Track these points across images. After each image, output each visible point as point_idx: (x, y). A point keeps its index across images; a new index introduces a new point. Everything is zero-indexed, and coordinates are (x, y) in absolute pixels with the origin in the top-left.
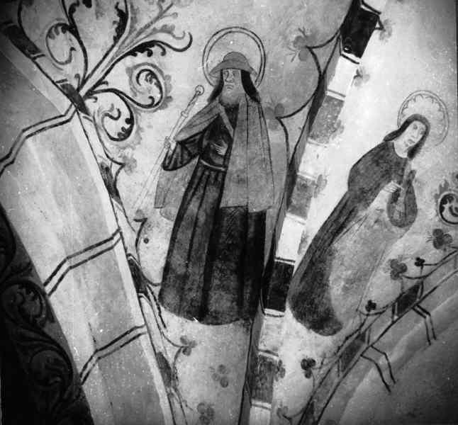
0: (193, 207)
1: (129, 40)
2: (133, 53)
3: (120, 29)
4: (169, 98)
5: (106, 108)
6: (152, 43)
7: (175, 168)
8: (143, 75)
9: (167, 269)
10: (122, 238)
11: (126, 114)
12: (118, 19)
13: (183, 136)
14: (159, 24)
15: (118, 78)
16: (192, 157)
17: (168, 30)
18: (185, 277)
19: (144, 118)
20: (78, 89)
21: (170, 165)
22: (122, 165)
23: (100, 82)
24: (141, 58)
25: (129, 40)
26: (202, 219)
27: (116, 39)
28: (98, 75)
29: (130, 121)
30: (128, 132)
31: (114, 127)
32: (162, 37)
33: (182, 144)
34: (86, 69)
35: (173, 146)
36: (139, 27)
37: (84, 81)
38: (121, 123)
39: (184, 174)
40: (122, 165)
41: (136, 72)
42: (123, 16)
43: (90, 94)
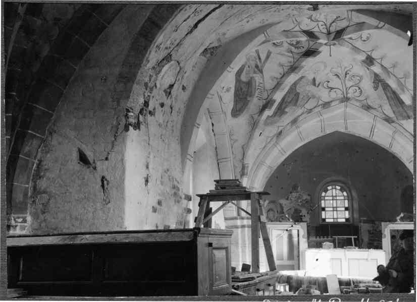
0: (389, 94)
1: (342, 76)
2: (346, 77)
3: (338, 76)
4: (362, 76)
5: (353, 92)
6: (346, 72)
7: (377, 89)
8: (352, 78)
9: (394, 112)
10: (377, 116)
11: (357, 88)
12: (335, 76)
13: (373, 81)
14: (343, 69)
15: (349, 84)
16: (378, 83)
17: (345, 68)
18: (399, 112)
19: (362, 85)
20: (344, 96)
21: (376, 88)
22: (366, 99)
23: (346, 89)
24: (348, 76)
25: (342, 76)
26: (393, 96)
27: (340, 79)
28: (345, 89)
29: (359, 88)
30: (361, 90)
31: (357, 94)
32: (346, 70)
33: (373, 82)
34: (341, 90)
35: (372, 84)
36: (341, 72)
37: (343, 93)
38: (358, 91)
39: (380, 88)
40: (366, 99)
41: (350, 79)
42: (336, 75)
43: (347, 94)
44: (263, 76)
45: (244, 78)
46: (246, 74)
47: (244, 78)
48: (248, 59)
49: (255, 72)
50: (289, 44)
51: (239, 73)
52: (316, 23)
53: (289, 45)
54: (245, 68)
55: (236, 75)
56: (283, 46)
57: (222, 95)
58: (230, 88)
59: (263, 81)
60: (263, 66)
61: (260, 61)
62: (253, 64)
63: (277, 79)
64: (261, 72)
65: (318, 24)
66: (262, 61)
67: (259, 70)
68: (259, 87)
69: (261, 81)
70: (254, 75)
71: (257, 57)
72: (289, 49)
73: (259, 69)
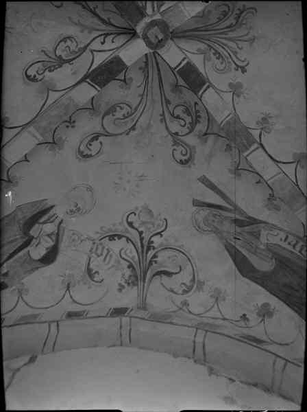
44: (265, 222)
45: (265, 265)
46: (255, 253)
47: (265, 265)
48: (216, 231)
49: (257, 236)
50: (190, 132)
51: (244, 267)
52: (88, 50)
53: (191, 134)
54: (238, 247)
55: (243, 276)
56: (194, 147)
57: (257, 330)
58: (266, 305)
59: (281, 230)
60: (242, 212)
61: (230, 211)
62: (228, 227)
63: (272, 197)
64: (253, 221)
65: (92, 51)
66: (227, 206)
67: (252, 224)
68: (298, 248)
69: (283, 235)
70: (263, 239)
71: (215, 211)
72: (199, 137)
73: (247, 223)
